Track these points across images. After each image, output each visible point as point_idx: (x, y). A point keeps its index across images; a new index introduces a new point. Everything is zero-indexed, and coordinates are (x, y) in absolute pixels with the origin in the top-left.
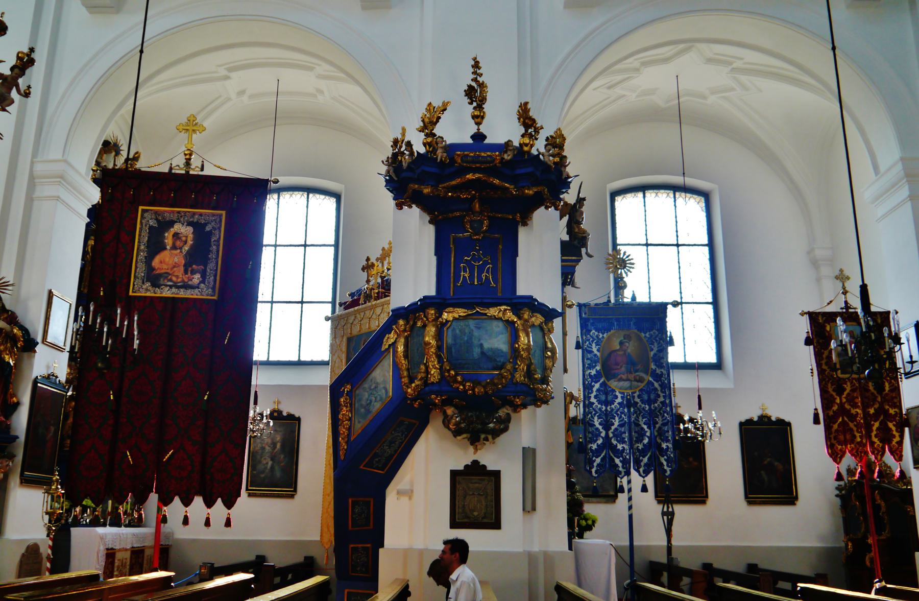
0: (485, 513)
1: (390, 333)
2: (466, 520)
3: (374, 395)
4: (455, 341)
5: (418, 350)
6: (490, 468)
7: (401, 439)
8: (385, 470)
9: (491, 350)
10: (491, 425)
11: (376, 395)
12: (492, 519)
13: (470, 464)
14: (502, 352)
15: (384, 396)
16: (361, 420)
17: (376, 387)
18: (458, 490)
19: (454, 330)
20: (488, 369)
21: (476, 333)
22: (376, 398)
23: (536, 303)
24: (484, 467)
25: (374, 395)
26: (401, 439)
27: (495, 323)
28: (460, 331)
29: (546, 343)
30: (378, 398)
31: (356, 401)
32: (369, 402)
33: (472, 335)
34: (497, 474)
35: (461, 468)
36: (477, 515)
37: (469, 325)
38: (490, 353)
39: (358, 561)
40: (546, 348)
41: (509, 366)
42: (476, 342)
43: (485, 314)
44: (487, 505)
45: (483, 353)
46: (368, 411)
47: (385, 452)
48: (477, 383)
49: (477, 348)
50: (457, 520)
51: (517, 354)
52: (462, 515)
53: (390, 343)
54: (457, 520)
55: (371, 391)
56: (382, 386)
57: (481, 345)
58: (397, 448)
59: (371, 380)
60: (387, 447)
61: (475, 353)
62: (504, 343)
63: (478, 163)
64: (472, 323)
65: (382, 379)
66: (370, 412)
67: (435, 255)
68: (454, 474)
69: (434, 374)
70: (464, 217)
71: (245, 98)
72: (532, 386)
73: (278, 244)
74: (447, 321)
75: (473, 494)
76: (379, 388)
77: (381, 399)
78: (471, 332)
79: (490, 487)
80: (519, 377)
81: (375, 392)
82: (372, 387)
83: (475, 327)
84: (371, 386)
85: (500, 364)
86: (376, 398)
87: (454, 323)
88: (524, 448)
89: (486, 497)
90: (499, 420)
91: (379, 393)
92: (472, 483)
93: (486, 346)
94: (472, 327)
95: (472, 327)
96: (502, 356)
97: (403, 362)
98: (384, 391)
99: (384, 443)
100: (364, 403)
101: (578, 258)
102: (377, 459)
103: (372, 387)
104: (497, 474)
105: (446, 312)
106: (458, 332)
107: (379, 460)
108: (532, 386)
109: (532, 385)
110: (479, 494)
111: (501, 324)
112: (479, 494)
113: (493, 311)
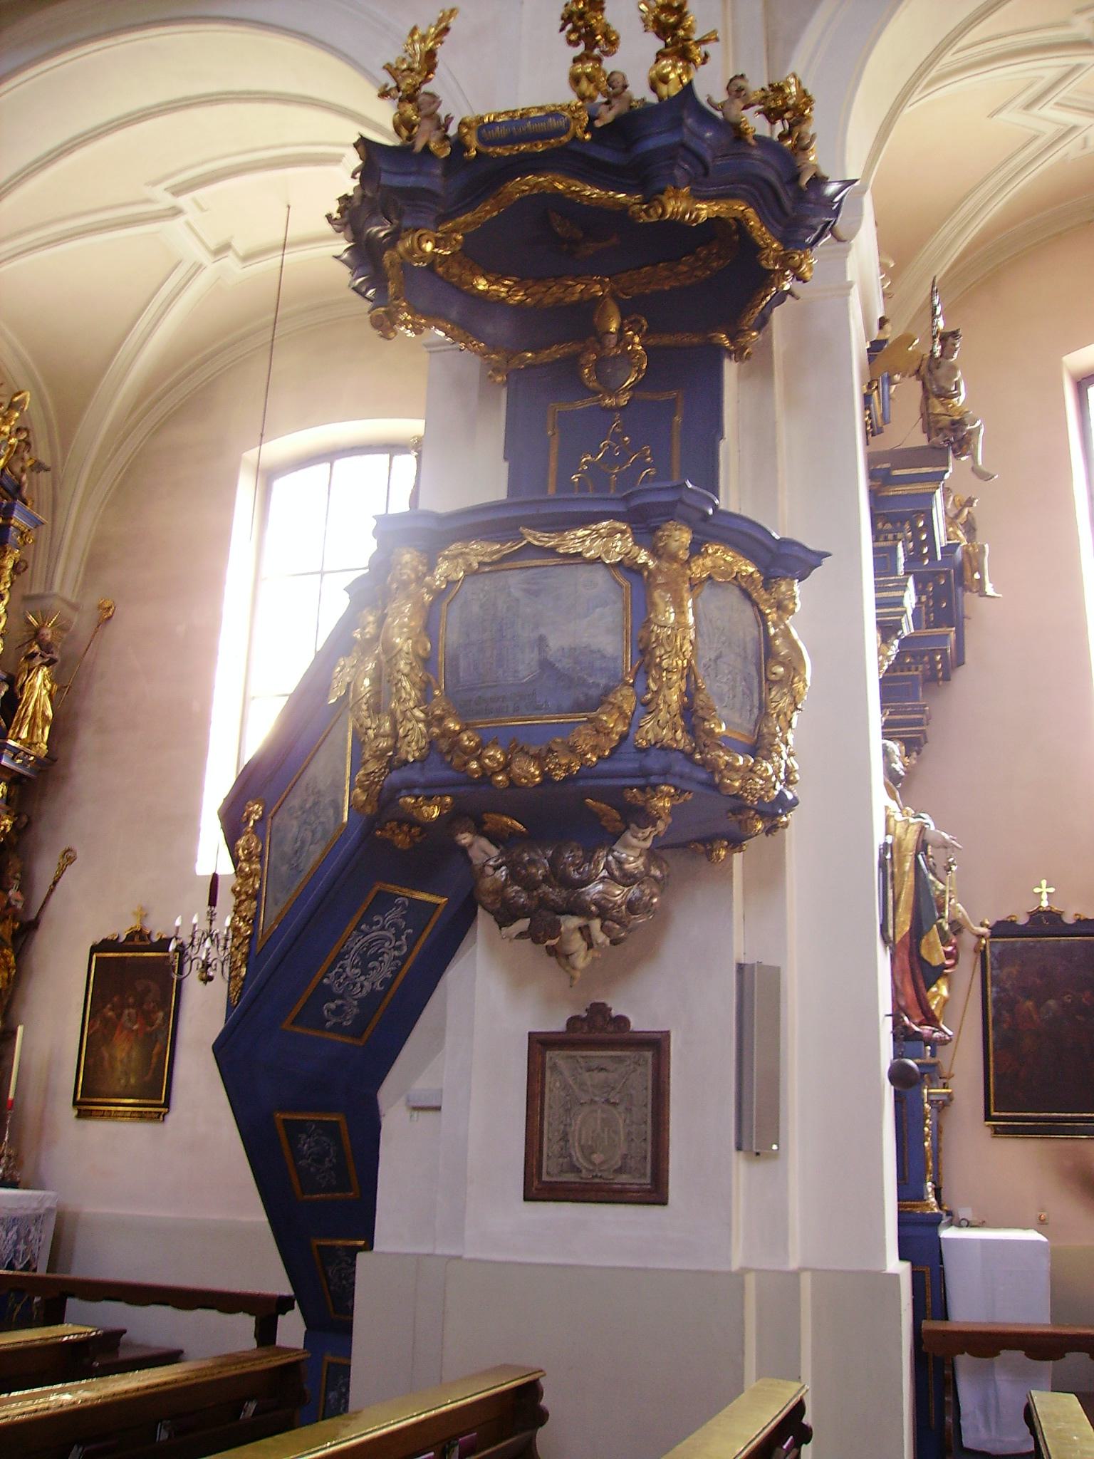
0: (625, 1157)
2: (570, 1177)
3: (310, 824)
6: (639, 1023)
7: (398, 948)
8: (366, 1036)
10: (595, 889)
12: (644, 1175)
13: (584, 1015)
14: (603, 657)
18: (551, 1091)
20: (560, 710)
22: (313, 832)
23: (711, 511)
24: (622, 1021)
25: (310, 824)
26: (398, 948)
27: (583, 573)
29: (768, 640)
30: (319, 835)
32: (298, 844)
34: (657, 1045)
35: (556, 1024)
36: (603, 1163)
38: (564, 664)
39: (344, 1282)
40: (767, 651)
41: (626, 699)
43: (552, 551)
44: (629, 1133)
46: (296, 869)
47: (355, 985)
48: (514, 749)
50: (545, 1178)
51: (647, 658)
52: (561, 1160)
54: (545, 1178)
56: (327, 800)
57: (542, 640)
58: (390, 976)
59: (307, 789)
60: (358, 971)
61: (521, 667)
63: (525, 142)
64: (515, 581)
67: (505, 459)
68: (540, 1044)
69: (406, 736)
70: (577, 356)
71: (230, 261)
72: (698, 757)
73: (325, 569)
74: (451, 583)
75: (592, 1102)
79: (642, 1079)
80: (655, 729)
83: (527, 591)
85: (594, 693)
86: (313, 832)
88: (741, 967)
89: (628, 1110)
90: (617, 873)
91: (322, 819)
92: (589, 1070)
93: (556, 642)
94: (516, 593)
95: (516, 593)
99: (341, 956)
100: (288, 848)
101: (937, 469)
102: (332, 1006)
104: (657, 1045)
105: (446, 558)
107: (338, 1007)
108: (698, 757)
109: (701, 753)
110: (607, 1101)
111: (600, 577)
112: (607, 1101)
113: (578, 540)
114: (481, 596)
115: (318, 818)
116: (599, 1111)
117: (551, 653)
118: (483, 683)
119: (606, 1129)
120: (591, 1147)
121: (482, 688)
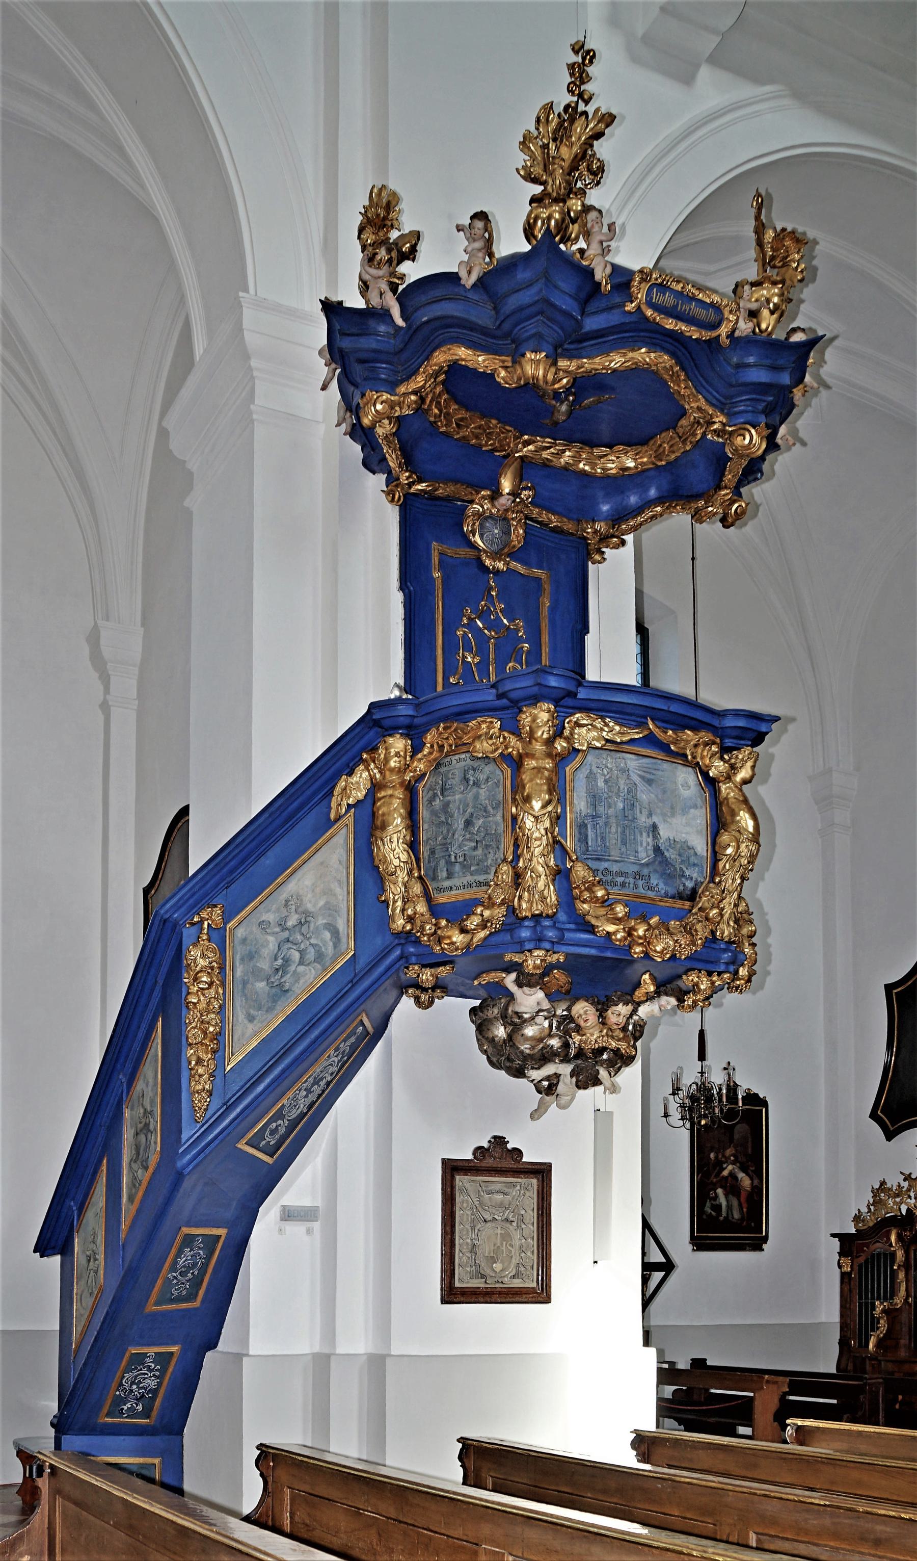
1: (351, 773)
4: (595, 806)
5: (468, 823)
9: (672, 843)
11: (302, 946)
14: (696, 854)
15: (329, 950)
16: (252, 1012)
17: (301, 924)
19: (591, 777)
21: (645, 795)
22: (302, 953)
28: (606, 781)
30: (311, 954)
31: (238, 957)
32: (280, 962)
33: (635, 798)
37: (628, 771)
42: (643, 820)
45: (657, 850)
46: (281, 991)
49: (644, 834)
53: (351, 801)
55: (286, 934)
56: (321, 921)
57: (654, 827)
61: (640, 849)
62: (699, 832)
65: (321, 903)
66: (287, 991)
76: (312, 925)
77: (320, 957)
78: (632, 790)
81: (299, 937)
82: (291, 923)
84: (285, 919)
87: (589, 758)
91: (313, 941)
93: (665, 832)
96: (694, 865)
97: (404, 857)
98: (327, 935)
100: (264, 965)
103: (291, 923)
106: (601, 783)
114: (605, 772)
115: (309, 939)
116: (499, 1228)
117: (662, 841)
118: (609, 856)
119: (504, 1243)
120: (492, 1258)
121: (608, 860)
